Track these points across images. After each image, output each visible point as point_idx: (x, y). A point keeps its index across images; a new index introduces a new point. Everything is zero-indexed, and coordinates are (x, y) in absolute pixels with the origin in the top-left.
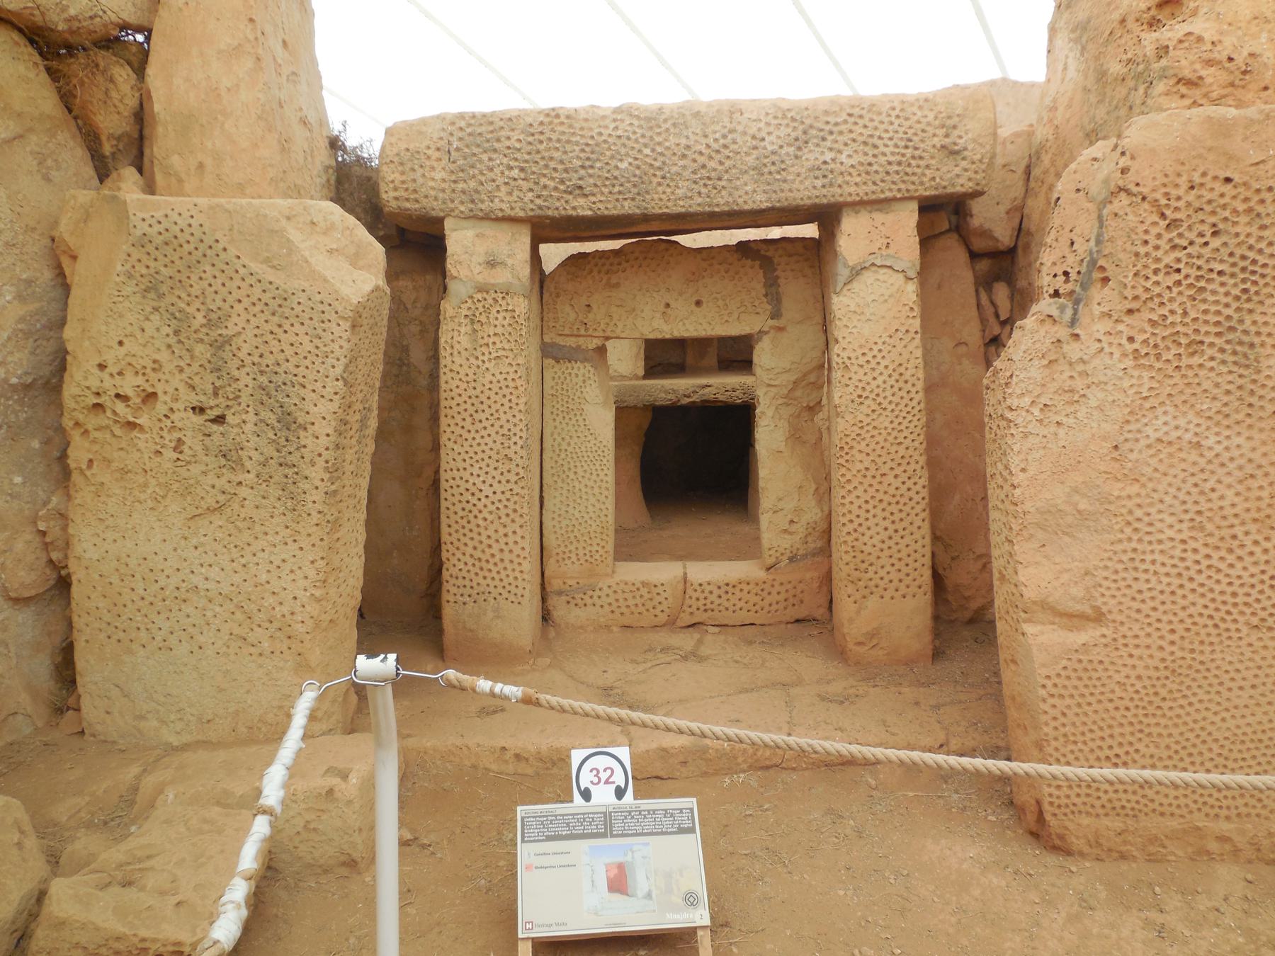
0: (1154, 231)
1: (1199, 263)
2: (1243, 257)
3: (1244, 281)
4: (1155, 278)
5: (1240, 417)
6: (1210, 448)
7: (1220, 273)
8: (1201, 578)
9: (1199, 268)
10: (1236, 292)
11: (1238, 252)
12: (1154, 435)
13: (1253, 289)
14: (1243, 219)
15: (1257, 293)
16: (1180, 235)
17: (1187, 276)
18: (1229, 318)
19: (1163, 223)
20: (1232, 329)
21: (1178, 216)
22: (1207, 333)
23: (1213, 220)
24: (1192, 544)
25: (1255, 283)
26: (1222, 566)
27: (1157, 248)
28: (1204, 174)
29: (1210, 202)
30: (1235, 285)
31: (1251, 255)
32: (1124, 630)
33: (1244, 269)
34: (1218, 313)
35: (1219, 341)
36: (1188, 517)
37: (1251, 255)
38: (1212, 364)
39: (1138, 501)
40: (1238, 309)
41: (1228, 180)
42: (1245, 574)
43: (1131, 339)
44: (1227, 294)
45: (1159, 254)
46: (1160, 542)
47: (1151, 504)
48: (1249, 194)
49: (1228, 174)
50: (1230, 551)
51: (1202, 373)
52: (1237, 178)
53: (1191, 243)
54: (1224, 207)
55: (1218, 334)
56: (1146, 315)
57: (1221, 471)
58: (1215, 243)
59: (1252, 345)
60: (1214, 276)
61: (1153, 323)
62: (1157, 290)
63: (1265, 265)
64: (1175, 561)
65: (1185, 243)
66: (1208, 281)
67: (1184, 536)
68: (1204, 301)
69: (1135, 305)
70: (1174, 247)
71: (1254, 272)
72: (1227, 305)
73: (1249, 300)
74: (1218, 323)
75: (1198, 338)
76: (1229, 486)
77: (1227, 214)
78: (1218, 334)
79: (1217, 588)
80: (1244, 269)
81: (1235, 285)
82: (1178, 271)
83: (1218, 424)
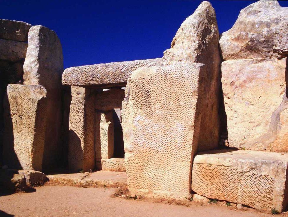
0: (135, 86)
1: (141, 91)
2: (147, 90)
3: (148, 94)
4: (135, 94)
5: (150, 117)
6: (146, 122)
7: (145, 93)
8: (147, 145)
9: (142, 92)
10: (147, 96)
11: (147, 89)
12: (138, 120)
13: (149, 95)
14: (147, 84)
15: (150, 96)
16: (138, 87)
17: (140, 94)
18: (146, 100)
19: (136, 85)
20: (147, 102)
21: (137, 84)
22: (144, 103)
23: (142, 84)
24: (145, 139)
25: (149, 94)
26: (150, 142)
27: (135, 89)
28: (140, 78)
29: (141, 82)
30: (147, 95)
31: (148, 90)
32: (136, 153)
33: (148, 92)
34: (145, 99)
35: (146, 104)
36: (144, 134)
37: (148, 90)
38: (145, 108)
39: (137, 131)
40: (148, 99)
41: (144, 78)
42: (154, 144)
43: (133, 104)
44: (146, 96)
45: (136, 90)
46: (140, 138)
47: (138, 132)
48: (147, 80)
49: (144, 78)
50: (151, 140)
51: (144, 109)
52: (145, 78)
53: (140, 88)
54: (144, 82)
55: (146, 103)
56: (135, 100)
57: (148, 126)
58: (143, 88)
59: (150, 105)
60: (144, 93)
61: (136, 101)
62: (136, 96)
63: (150, 92)
64: (143, 142)
65: (139, 88)
66: (143, 94)
67: (144, 137)
68: (143, 97)
69: (133, 98)
70: (138, 89)
71: (149, 93)
72: (146, 98)
73: (149, 97)
74: (145, 101)
75: (143, 103)
76: (150, 128)
77: (144, 83)
78: (146, 103)
79: (150, 146)
80: (148, 92)
81: (147, 95)
82: (139, 93)
83: (147, 118)
